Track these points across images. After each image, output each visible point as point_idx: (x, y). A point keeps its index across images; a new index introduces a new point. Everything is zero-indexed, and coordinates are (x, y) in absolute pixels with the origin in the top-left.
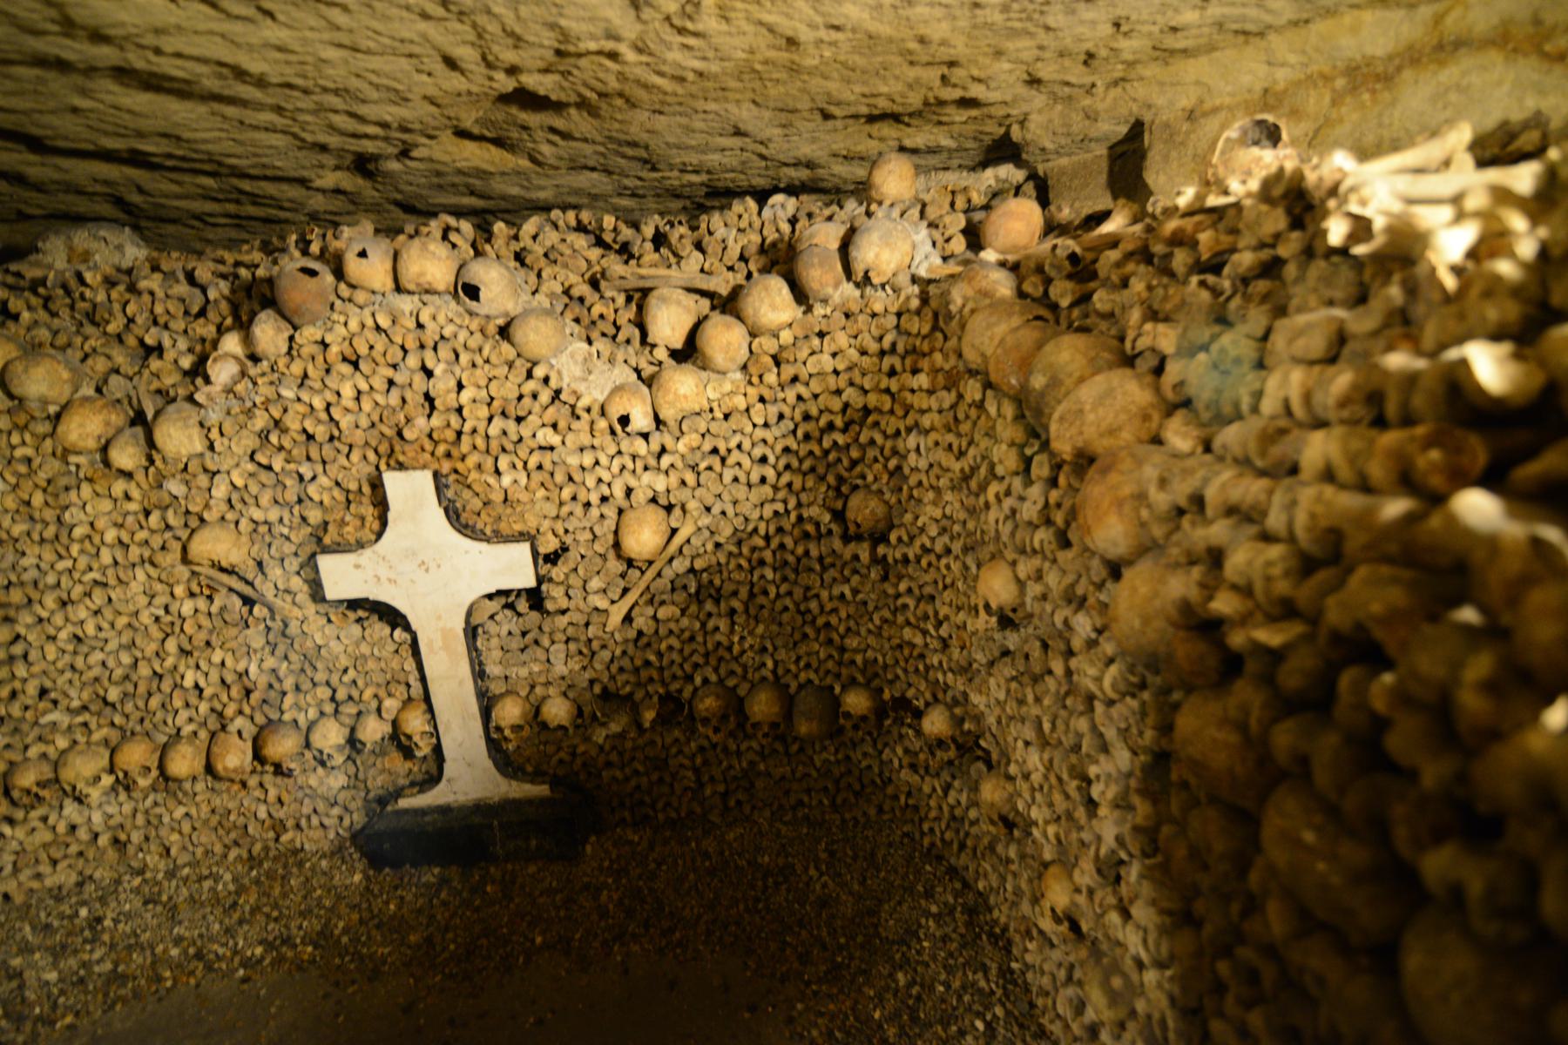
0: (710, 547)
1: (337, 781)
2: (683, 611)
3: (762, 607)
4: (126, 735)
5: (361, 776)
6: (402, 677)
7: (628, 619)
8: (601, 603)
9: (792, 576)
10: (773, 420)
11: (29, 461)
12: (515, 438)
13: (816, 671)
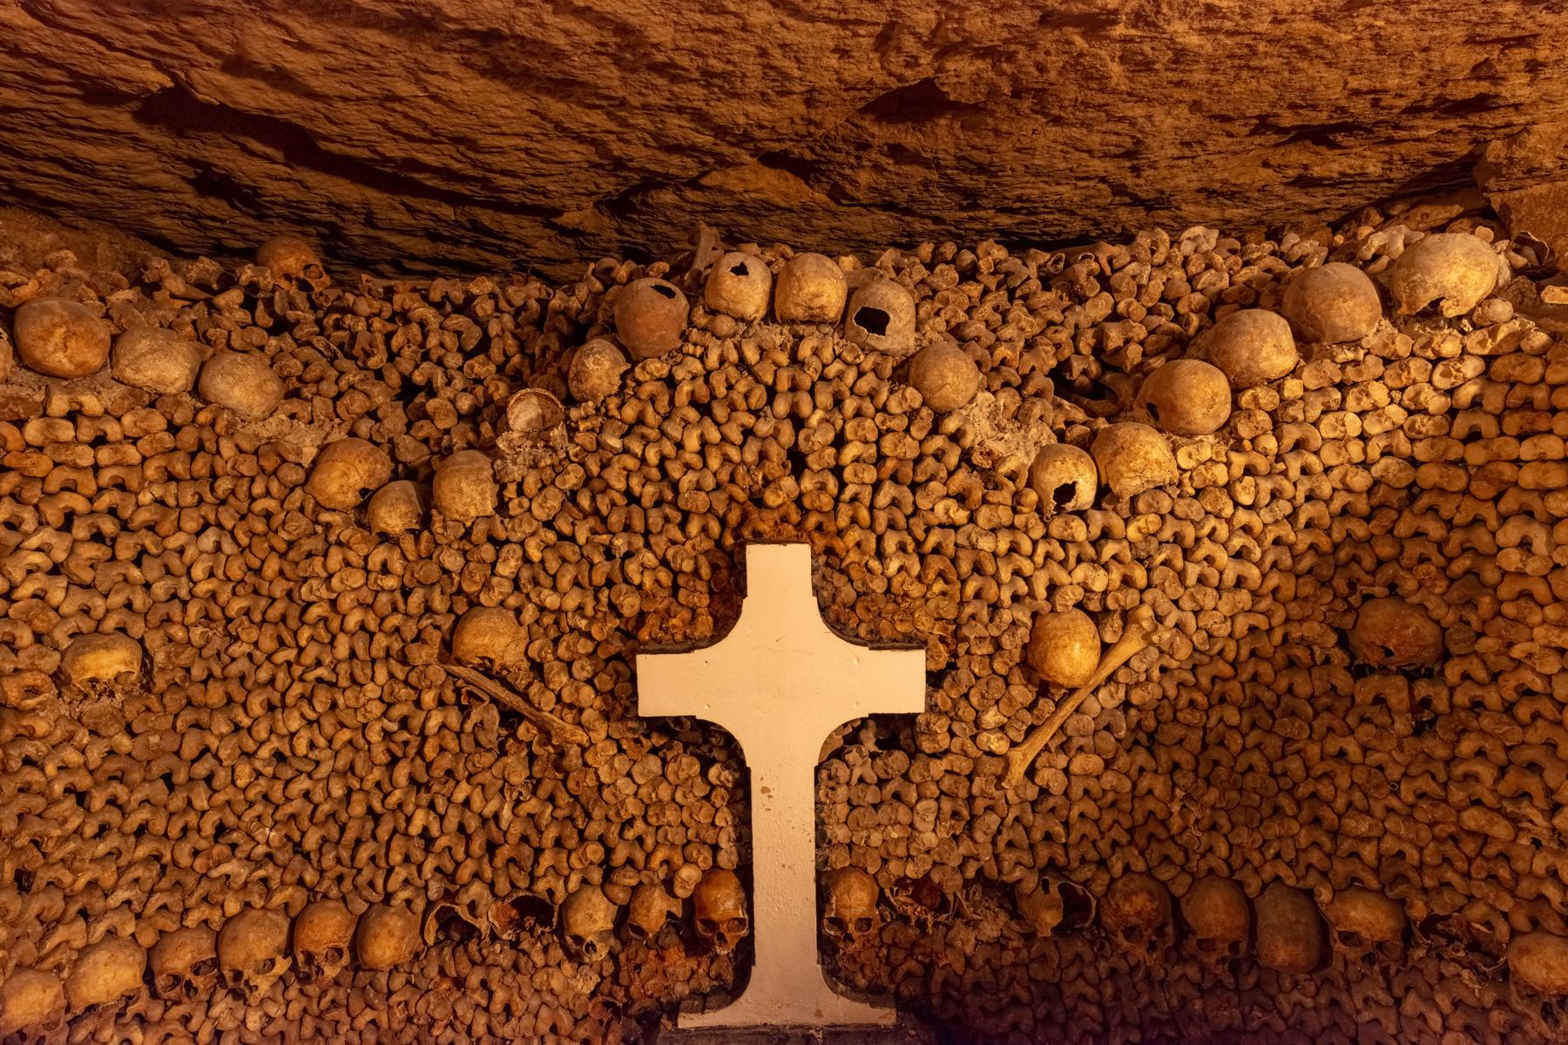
0: (1156, 674)
1: (585, 986)
2: (1108, 764)
3: (1216, 763)
4: (314, 897)
5: (624, 980)
6: (709, 835)
7: (1031, 773)
8: (998, 745)
9: (1266, 721)
10: (1265, 498)
11: (268, 516)
12: (909, 510)
13: (1289, 864)
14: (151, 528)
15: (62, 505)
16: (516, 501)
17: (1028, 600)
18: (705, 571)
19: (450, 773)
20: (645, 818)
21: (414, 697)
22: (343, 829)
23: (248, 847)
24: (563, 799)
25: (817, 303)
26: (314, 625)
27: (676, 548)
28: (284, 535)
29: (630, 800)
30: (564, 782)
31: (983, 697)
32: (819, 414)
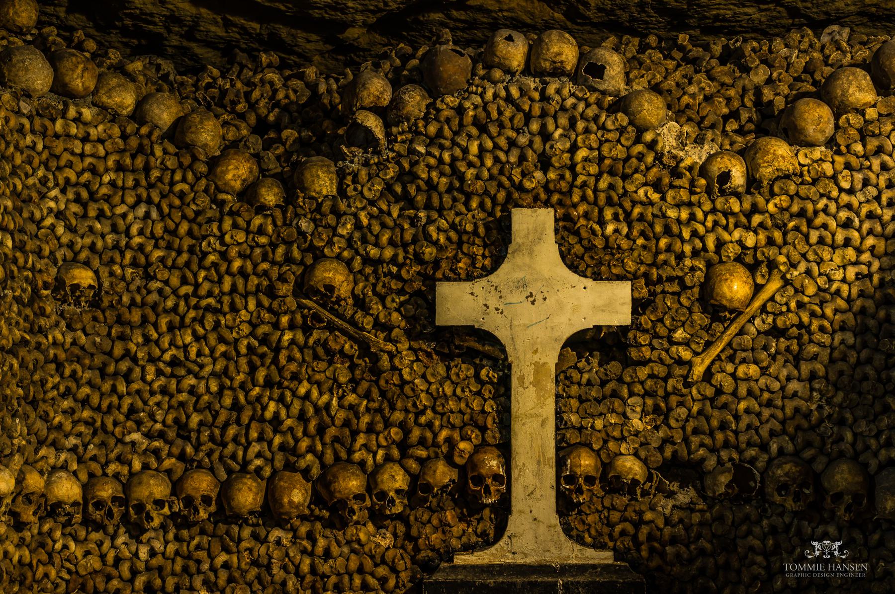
0: (793, 305)
5: (414, 532)
7: (708, 375)
11: (182, 195)
14: (107, 199)
15: (65, 175)
16: (352, 187)
17: (702, 253)
18: (481, 230)
19: (295, 377)
21: (274, 320)
22: (215, 416)
24: (375, 394)
25: (558, 59)
26: (208, 269)
27: (461, 217)
28: (194, 207)
29: (423, 396)
30: (377, 382)
31: (673, 319)
32: (560, 131)
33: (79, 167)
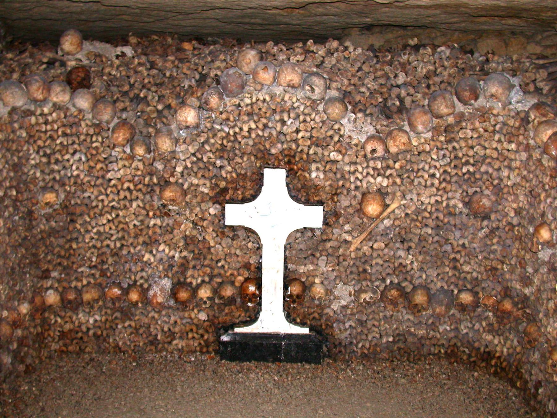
2: (386, 245)
11: (97, 148)
20: (225, 260)
23: (89, 263)
25: (292, 83)
33: (44, 139)
